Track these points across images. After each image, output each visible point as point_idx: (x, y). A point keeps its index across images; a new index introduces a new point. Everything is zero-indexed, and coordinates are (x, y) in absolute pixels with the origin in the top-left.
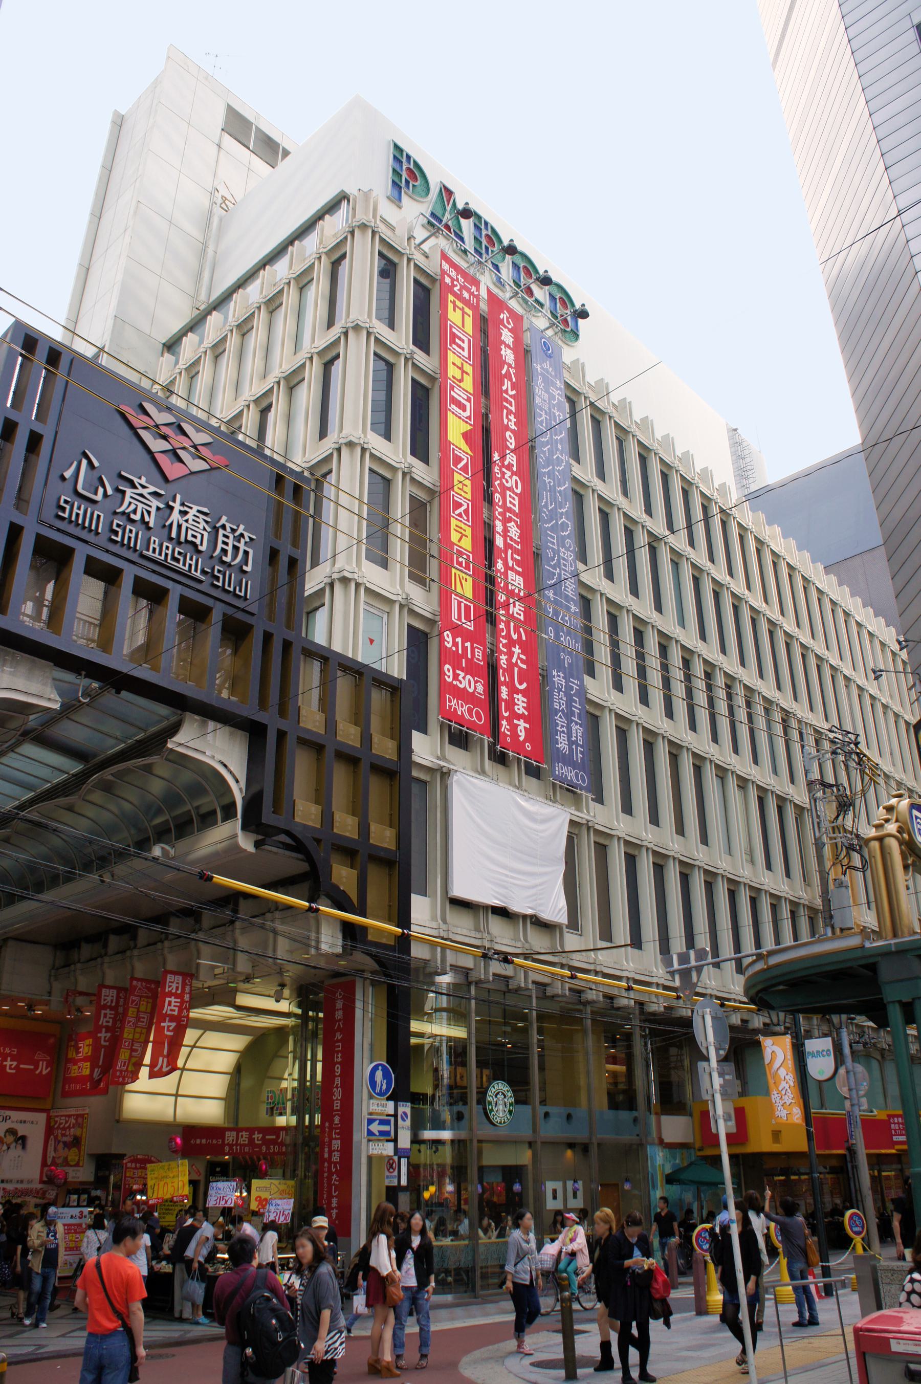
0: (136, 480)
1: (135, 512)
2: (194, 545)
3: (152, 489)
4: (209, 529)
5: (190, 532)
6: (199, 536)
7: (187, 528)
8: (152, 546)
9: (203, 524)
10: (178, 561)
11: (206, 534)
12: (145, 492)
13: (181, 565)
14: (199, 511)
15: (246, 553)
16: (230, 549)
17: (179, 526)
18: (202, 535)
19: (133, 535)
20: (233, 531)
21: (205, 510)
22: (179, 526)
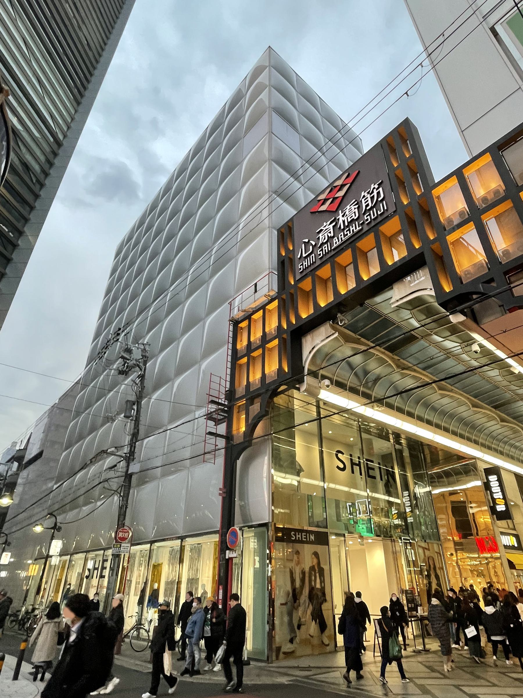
0: (322, 228)
1: (325, 239)
2: (353, 219)
3: (329, 223)
4: (357, 206)
5: (349, 218)
6: (353, 215)
7: (347, 218)
8: (335, 242)
9: (353, 208)
10: (347, 235)
11: (356, 210)
12: (327, 227)
13: (349, 235)
14: (350, 206)
15: (378, 193)
16: (370, 202)
17: (344, 222)
18: (355, 212)
19: (326, 248)
20: (368, 193)
21: (354, 200)
22: (344, 222)
